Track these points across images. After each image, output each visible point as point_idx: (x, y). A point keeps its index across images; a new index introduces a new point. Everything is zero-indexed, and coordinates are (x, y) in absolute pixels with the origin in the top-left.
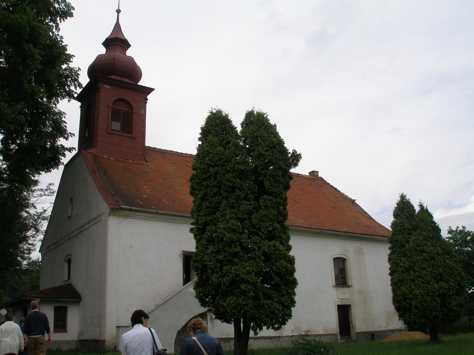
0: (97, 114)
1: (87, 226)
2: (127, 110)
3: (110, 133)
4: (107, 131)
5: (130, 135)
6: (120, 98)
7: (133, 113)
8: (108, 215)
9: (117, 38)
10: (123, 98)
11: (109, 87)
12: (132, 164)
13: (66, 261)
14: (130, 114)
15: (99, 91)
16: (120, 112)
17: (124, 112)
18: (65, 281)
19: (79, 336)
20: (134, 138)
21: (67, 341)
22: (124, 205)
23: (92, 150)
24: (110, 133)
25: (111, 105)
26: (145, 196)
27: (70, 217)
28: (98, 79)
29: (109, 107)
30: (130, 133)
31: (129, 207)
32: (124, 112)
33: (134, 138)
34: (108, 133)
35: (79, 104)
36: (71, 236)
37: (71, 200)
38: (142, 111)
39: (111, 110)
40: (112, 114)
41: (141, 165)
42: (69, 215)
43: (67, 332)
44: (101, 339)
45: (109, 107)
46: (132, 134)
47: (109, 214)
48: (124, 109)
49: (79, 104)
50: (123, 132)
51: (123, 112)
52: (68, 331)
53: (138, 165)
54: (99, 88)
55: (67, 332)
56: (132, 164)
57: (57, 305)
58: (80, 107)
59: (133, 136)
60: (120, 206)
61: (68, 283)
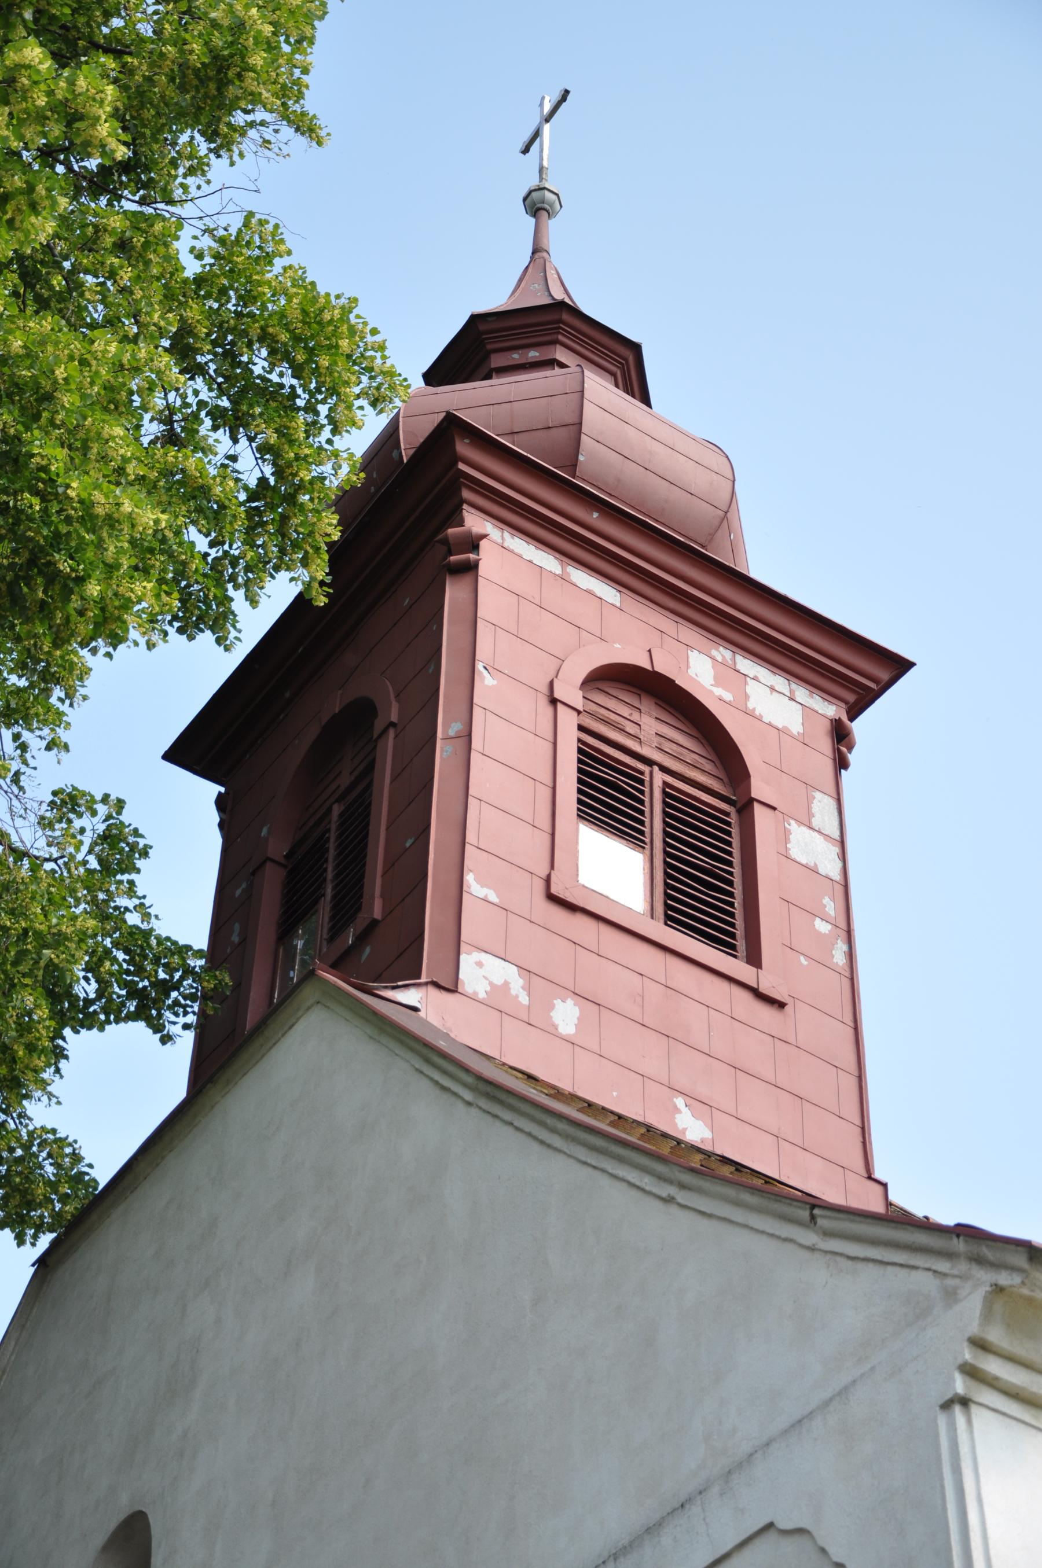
0: (456, 728)
4: (548, 880)
7: (746, 806)
8: (960, 1385)
10: (659, 668)
14: (727, 814)
15: (471, 568)
16: (642, 773)
17: (670, 779)
20: (781, 1005)
23: (409, 996)
24: (571, 907)
25: (570, 692)
28: (461, 466)
29: (554, 701)
33: (781, 1005)
38: (816, 807)
39: (568, 722)
40: (584, 778)
45: (554, 701)
46: (754, 959)
47: (971, 1372)
51: (665, 783)
54: (473, 543)
58: (221, 803)
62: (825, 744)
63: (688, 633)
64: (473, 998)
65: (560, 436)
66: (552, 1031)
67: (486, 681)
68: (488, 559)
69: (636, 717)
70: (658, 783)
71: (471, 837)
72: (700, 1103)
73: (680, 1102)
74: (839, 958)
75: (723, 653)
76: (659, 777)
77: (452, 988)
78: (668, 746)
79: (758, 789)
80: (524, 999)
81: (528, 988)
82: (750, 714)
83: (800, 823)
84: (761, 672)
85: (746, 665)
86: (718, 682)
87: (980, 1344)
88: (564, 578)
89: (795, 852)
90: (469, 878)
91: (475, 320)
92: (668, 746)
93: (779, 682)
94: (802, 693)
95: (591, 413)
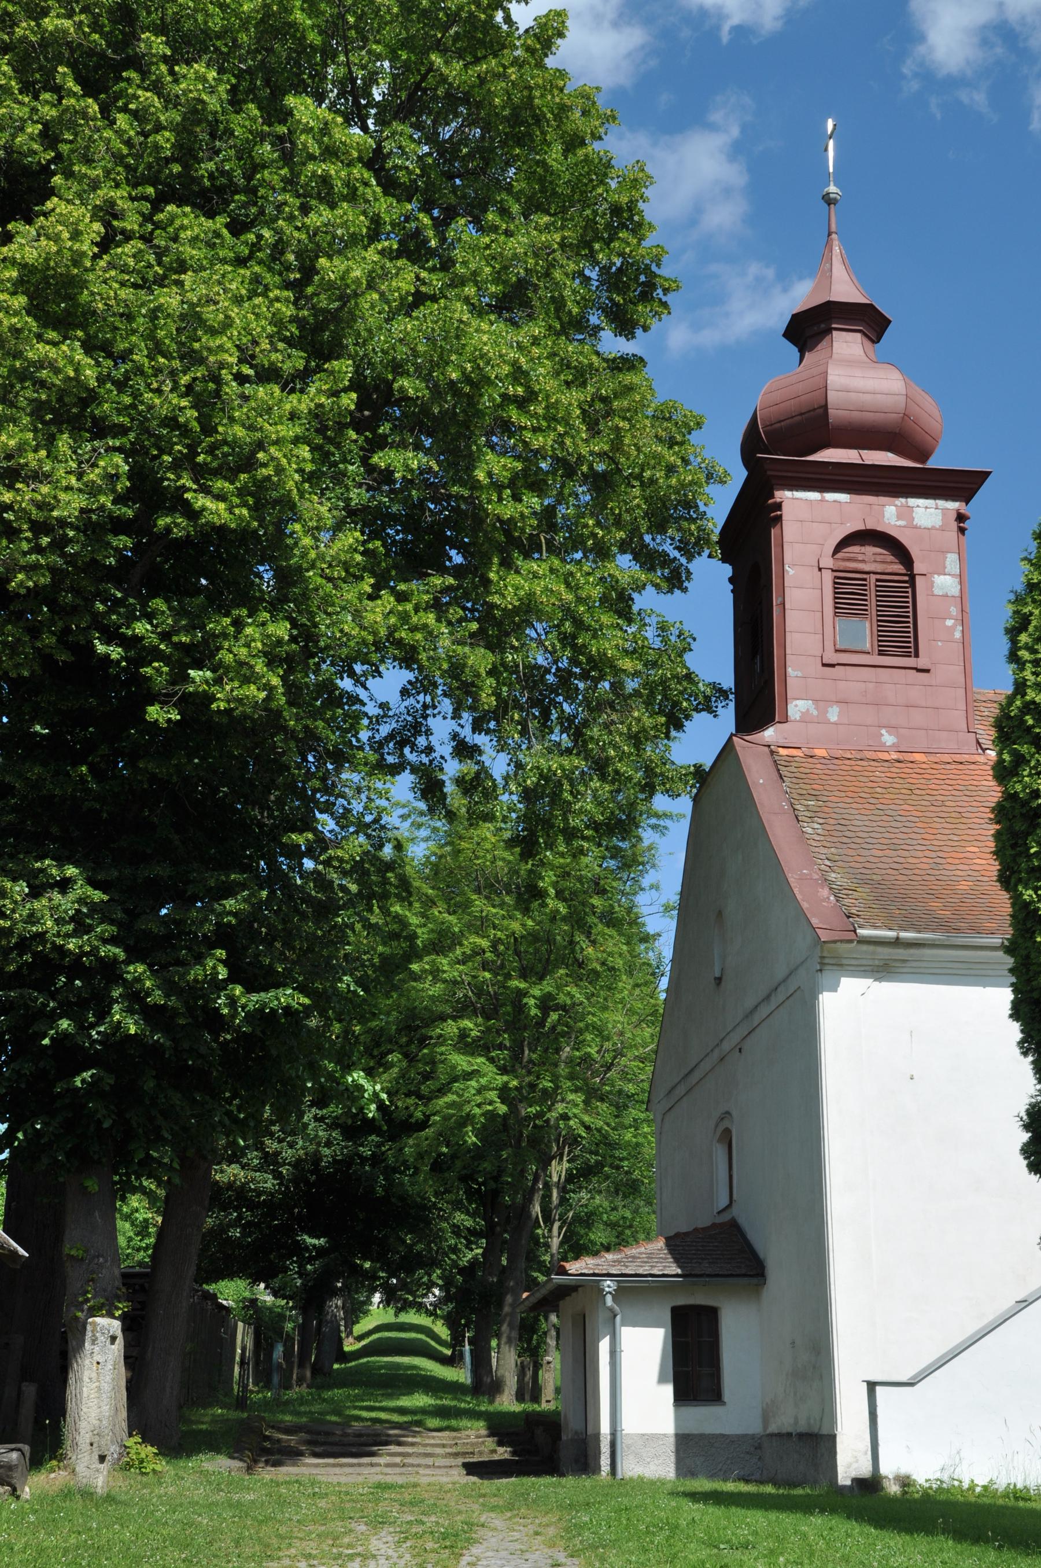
0: (780, 599)
1: (764, 1011)
2: (891, 568)
3: (832, 666)
5: (910, 662)
6: (861, 527)
9: (829, 303)
11: (814, 496)
12: (924, 766)
13: (720, 1141)
17: (879, 577)
18: (719, 1213)
19: (766, 1420)
20: (928, 671)
21: (723, 1436)
22: (876, 927)
23: (769, 734)
24: (832, 666)
25: (828, 562)
26: (964, 886)
27: (719, 980)
28: (769, 473)
29: (820, 569)
30: (908, 655)
31: (892, 934)
32: (879, 577)
33: (928, 671)
34: (824, 665)
35: (727, 570)
36: (726, 1046)
37: (720, 914)
38: (948, 563)
41: (960, 767)
42: (717, 975)
43: (724, 1403)
44: (824, 1431)
46: (917, 655)
48: (879, 568)
49: (727, 570)
50: (881, 653)
51: (878, 580)
52: (727, 1394)
53: (948, 766)
54: (779, 506)
55: (724, 1403)
56: (924, 766)
57: (682, 1301)
58: (731, 580)
59: (922, 662)
60: (855, 931)
61: (725, 1218)
62: (954, 525)
63: (882, 499)
64: (795, 721)
65: (821, 411)
66: (828, 722)
67: (790, 571)
68: (787, 512)
69: (863, 549)
70: (873, 581)
71: (788, 651)
72: (891, 728)
73: (883, 731)
74: (958, 635)
75: (901, 501)
76: (873, 577)
77: (785, 720)
78: (878, 558)
79: (918, 568)
80: (815, 713)
81: (817, 708)
82: (916, 527)
83: (939, 574)
84: (921, 502)
85: (912, 502)
86: (899, 517)
87: (822, 957)
88: (823, 500)
89: (937, 591)
90: (789, 670)
91: (794, 316)
92: (878, 558)
93: (930, 502)
94: (941, 503)
95: (831, 396)
